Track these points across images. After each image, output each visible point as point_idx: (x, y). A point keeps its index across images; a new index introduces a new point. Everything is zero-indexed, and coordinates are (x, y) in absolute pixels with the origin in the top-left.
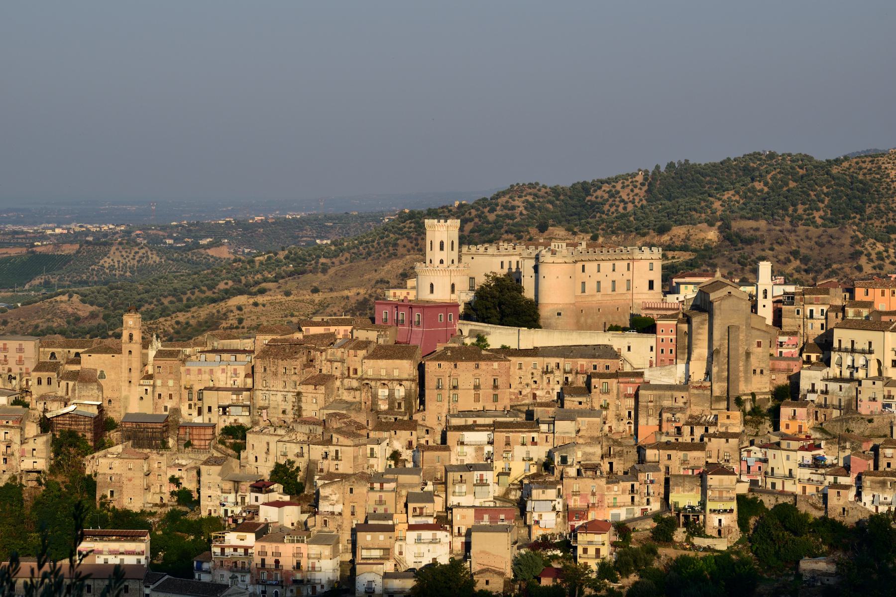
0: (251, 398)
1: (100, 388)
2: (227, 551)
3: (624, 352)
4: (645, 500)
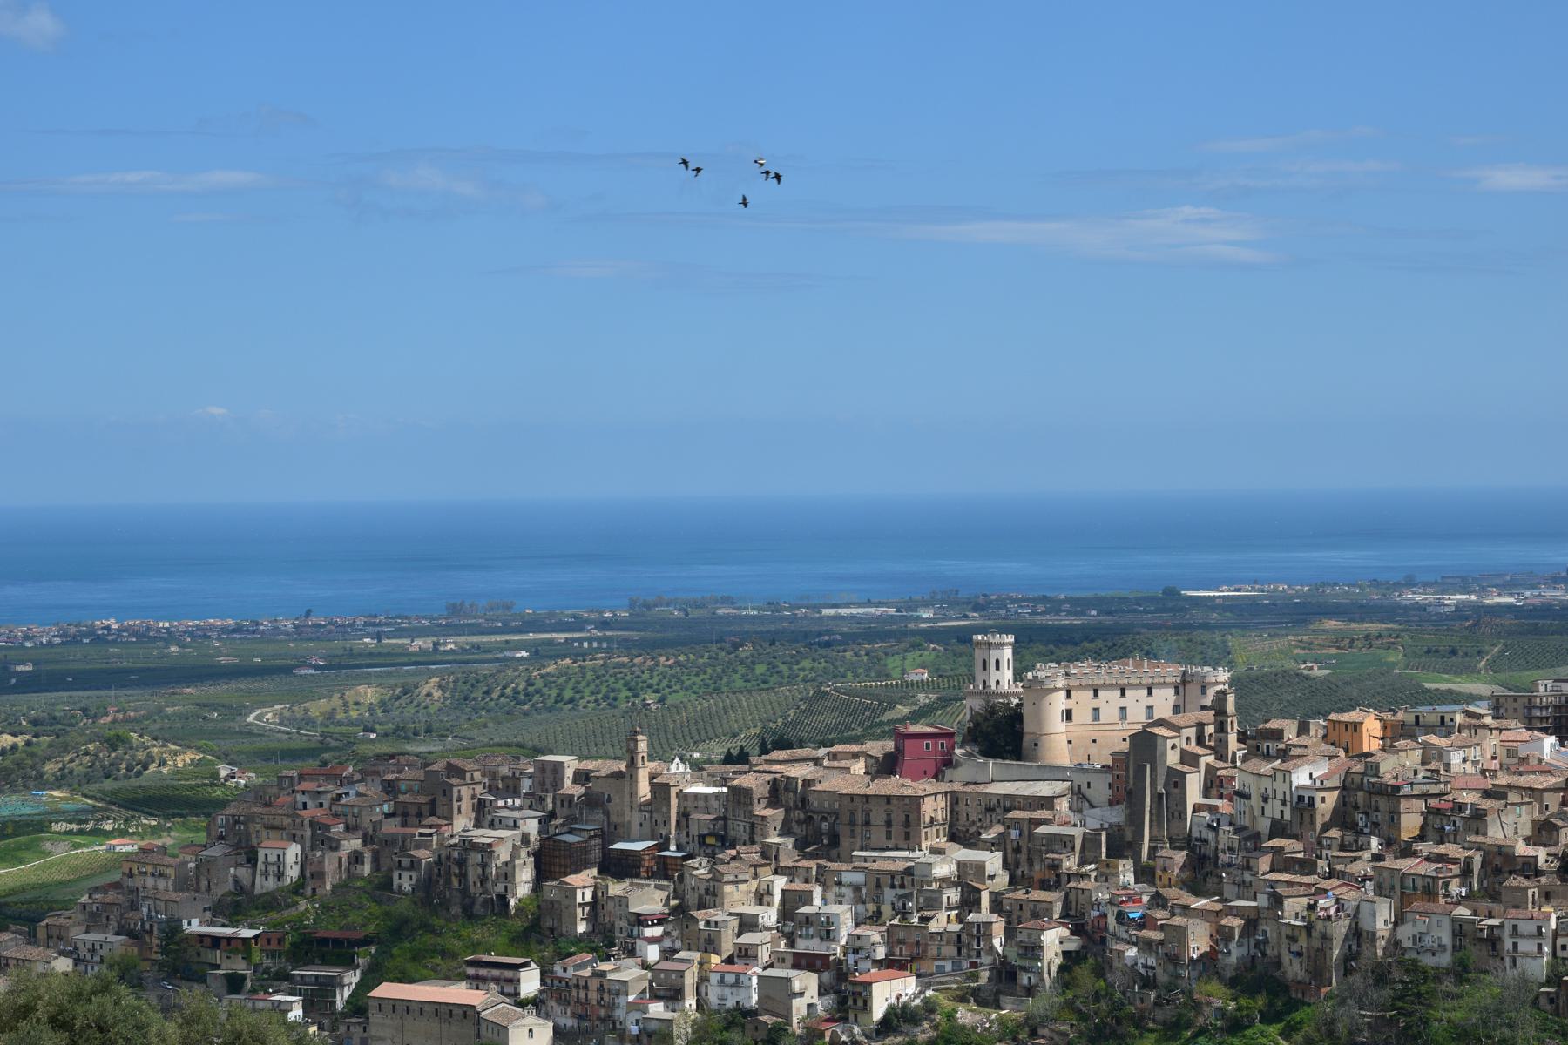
0: (725, 827)
1: (607, 814)
2: (556, 982)
3: (1084, 787)
4: (973, 953)
